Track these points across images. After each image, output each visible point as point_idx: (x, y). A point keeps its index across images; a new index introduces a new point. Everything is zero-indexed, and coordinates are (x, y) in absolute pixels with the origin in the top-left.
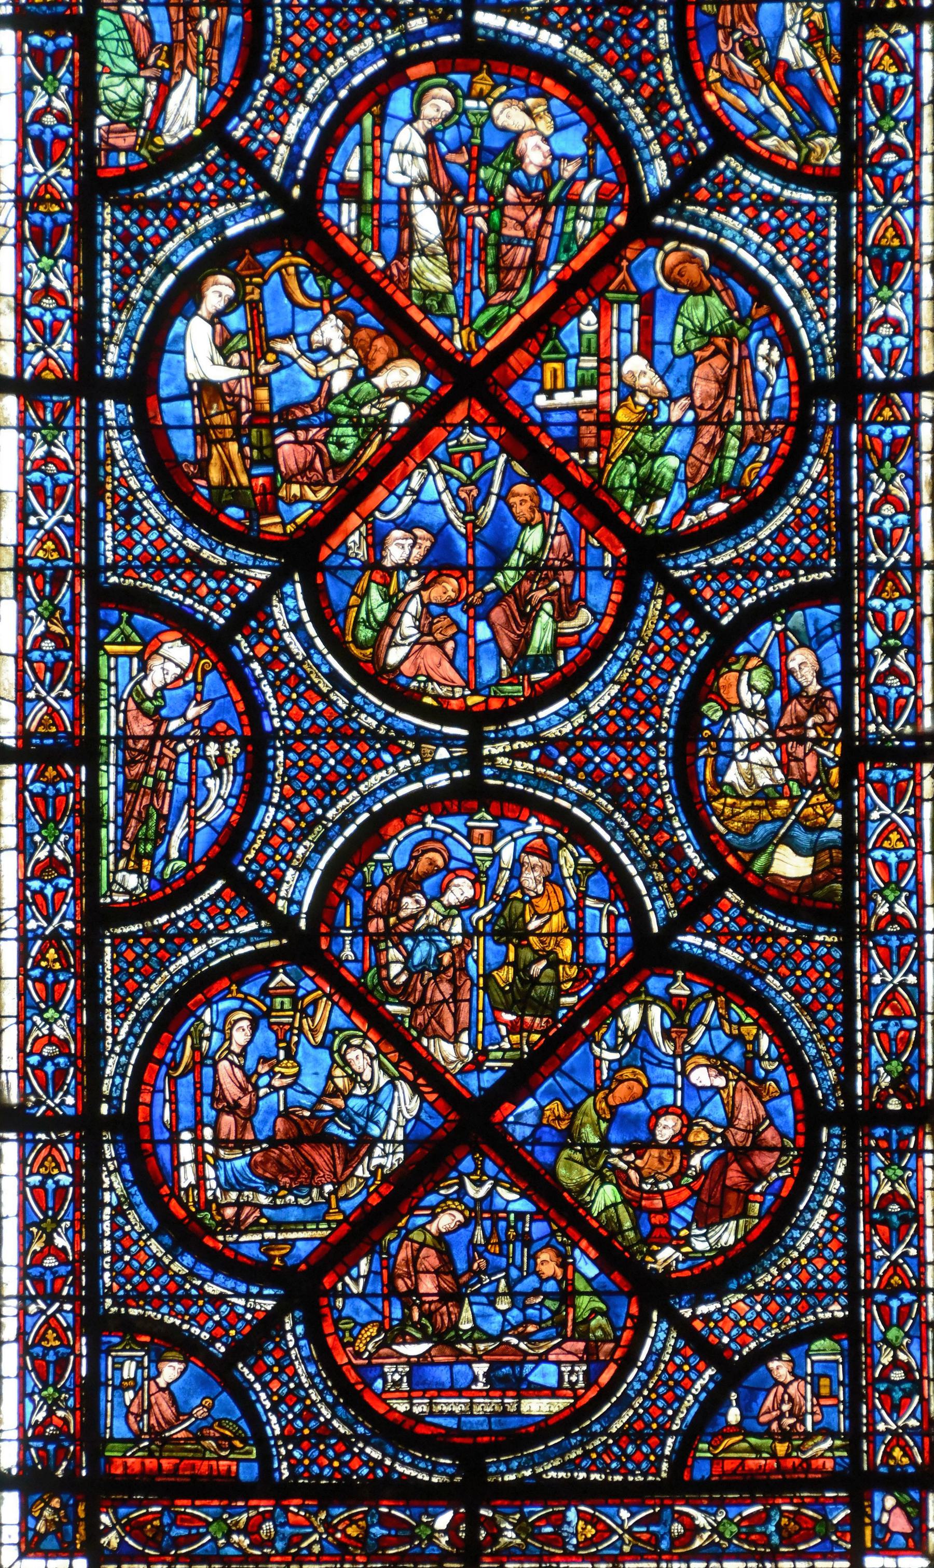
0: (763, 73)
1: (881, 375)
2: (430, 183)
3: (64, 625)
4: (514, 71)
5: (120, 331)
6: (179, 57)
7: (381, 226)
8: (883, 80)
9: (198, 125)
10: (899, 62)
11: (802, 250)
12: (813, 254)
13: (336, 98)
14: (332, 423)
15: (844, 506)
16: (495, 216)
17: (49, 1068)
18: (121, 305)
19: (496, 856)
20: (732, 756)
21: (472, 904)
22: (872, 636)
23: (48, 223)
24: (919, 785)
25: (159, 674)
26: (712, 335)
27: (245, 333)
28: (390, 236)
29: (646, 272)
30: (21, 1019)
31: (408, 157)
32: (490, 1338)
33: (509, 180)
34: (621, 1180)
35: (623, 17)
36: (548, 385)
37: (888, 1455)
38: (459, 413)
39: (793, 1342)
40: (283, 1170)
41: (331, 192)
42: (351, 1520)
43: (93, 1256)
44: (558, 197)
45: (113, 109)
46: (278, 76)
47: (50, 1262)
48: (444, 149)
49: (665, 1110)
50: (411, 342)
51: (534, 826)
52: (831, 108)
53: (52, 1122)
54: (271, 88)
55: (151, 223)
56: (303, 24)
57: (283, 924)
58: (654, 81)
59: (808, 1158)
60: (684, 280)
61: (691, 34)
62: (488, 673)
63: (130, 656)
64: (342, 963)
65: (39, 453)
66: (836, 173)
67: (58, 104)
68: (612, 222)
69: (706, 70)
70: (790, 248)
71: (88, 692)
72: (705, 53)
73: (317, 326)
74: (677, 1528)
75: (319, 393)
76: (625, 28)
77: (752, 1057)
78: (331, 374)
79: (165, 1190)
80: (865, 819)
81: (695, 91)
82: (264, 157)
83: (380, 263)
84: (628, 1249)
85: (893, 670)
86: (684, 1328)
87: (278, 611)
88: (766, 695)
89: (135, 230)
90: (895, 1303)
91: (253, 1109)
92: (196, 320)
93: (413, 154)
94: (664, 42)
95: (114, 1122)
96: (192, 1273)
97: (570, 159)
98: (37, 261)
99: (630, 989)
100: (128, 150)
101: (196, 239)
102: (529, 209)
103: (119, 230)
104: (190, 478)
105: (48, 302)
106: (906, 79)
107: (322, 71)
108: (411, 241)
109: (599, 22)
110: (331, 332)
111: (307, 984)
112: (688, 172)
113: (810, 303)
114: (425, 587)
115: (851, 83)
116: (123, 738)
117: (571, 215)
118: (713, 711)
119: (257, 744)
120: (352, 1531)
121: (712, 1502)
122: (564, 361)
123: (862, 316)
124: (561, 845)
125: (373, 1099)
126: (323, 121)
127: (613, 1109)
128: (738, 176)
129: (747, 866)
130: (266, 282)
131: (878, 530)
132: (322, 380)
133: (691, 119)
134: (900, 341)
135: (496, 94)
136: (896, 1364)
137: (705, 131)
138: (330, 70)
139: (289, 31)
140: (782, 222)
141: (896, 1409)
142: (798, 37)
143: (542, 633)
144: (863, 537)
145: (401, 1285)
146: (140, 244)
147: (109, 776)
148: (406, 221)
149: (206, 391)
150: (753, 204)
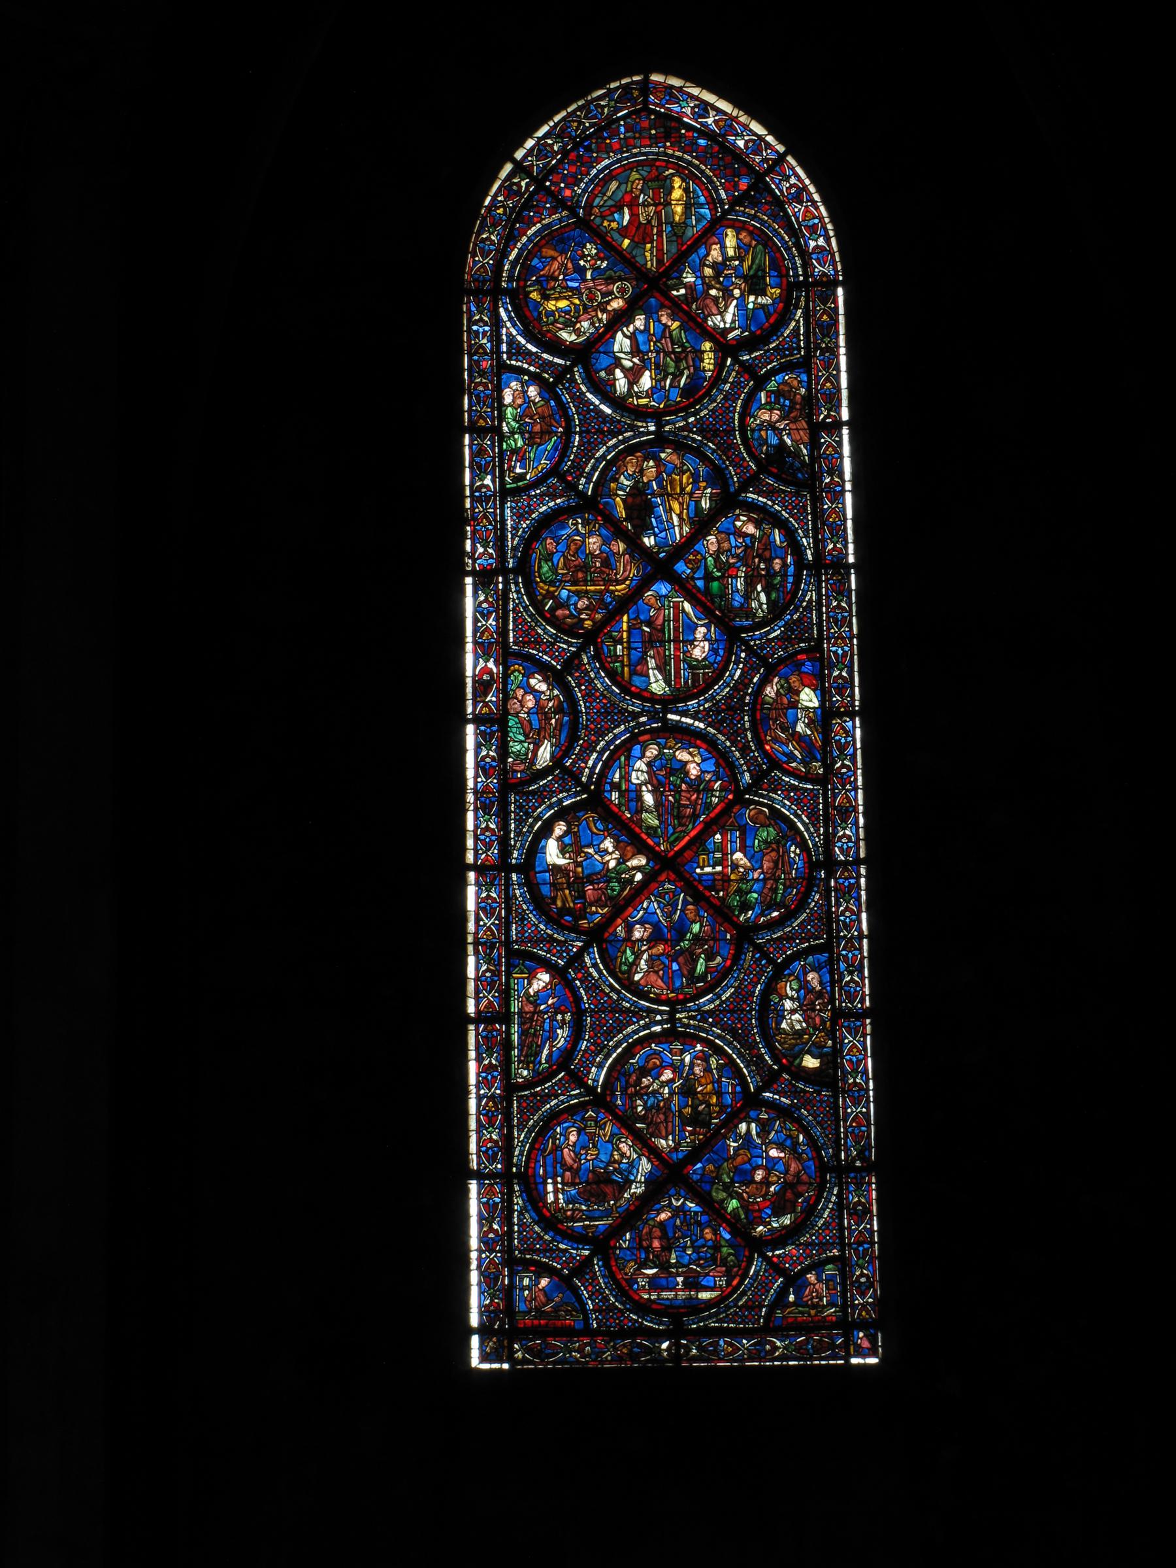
3: (495, 966)
5: (518, 845)
6: (542, 734)
7: (630, 800)
10: (847, 732)
14: (609, 881)
15: (829, 912)
17: (490, 1152)
18: (519, 833)
19: (682, 1060)
20: (784, 1017)
21: (672, 1081)
22: (843, 966)
24: (865, 1028)
25: (536, 986)
26: (770, 843)
30: (478, 1132)
32: (683, 1266)
33: (683, 781)
34: (739, 1197)
37: (860, 1314)
38: (663, 877)
39: (818, 1266)
40: (592, 1195)
41: (607, 787)
42: (624, 1346)
43: (510, 1232)
47: (491, 1235)
49: (759, 1167)
50: (641, 848)
51: (699, 1047)
53: (492, 1175)
57: (591, 1090)
59: (821, 1188)
62: (678, 984)
63: (524, 978)
64: (617, 1106)
65: (484, 895)
67: (492, 753)
71: (506, 995)
73: (602, 842)
74: (768, 1347)
77: (796, 1143)
79: (541, 1204)
80: (842, 1043)
81: (760, 745)
84: (743, 1227)
85: (852, 980)
86: (768, 1260)
87: (587, 959)
88: (798, 991)
90: (861, 1249)
91: (579, 1168)
94: (747, 725)
95: (519, 1175)
96: (553, 1240)
99: (741, 1116)
100: (521, 772)
101: (550, 807)
104: (548, 904)
108: (642, 806)
110: (608, 844)
111: (602, 1115)
114: (649, 948)
116: (521, 1013)
118: (775, 999)
119: (579, 1014)
120: (625, 1351)
121: (783, 1336)
123: (834, 834)
124: (711, 1056)
125: (632, 1164)
127: (736, 1167)
129: (792, 1063)
131: (844, 922)
134: (850, 844)
136: (862, 1275)
141: (863, 1295)
143: (701, 967)
144: (837, 925)
145: (644, 1244)
147: (515, 1028)
148: (639, 798)
149: (556, 869)
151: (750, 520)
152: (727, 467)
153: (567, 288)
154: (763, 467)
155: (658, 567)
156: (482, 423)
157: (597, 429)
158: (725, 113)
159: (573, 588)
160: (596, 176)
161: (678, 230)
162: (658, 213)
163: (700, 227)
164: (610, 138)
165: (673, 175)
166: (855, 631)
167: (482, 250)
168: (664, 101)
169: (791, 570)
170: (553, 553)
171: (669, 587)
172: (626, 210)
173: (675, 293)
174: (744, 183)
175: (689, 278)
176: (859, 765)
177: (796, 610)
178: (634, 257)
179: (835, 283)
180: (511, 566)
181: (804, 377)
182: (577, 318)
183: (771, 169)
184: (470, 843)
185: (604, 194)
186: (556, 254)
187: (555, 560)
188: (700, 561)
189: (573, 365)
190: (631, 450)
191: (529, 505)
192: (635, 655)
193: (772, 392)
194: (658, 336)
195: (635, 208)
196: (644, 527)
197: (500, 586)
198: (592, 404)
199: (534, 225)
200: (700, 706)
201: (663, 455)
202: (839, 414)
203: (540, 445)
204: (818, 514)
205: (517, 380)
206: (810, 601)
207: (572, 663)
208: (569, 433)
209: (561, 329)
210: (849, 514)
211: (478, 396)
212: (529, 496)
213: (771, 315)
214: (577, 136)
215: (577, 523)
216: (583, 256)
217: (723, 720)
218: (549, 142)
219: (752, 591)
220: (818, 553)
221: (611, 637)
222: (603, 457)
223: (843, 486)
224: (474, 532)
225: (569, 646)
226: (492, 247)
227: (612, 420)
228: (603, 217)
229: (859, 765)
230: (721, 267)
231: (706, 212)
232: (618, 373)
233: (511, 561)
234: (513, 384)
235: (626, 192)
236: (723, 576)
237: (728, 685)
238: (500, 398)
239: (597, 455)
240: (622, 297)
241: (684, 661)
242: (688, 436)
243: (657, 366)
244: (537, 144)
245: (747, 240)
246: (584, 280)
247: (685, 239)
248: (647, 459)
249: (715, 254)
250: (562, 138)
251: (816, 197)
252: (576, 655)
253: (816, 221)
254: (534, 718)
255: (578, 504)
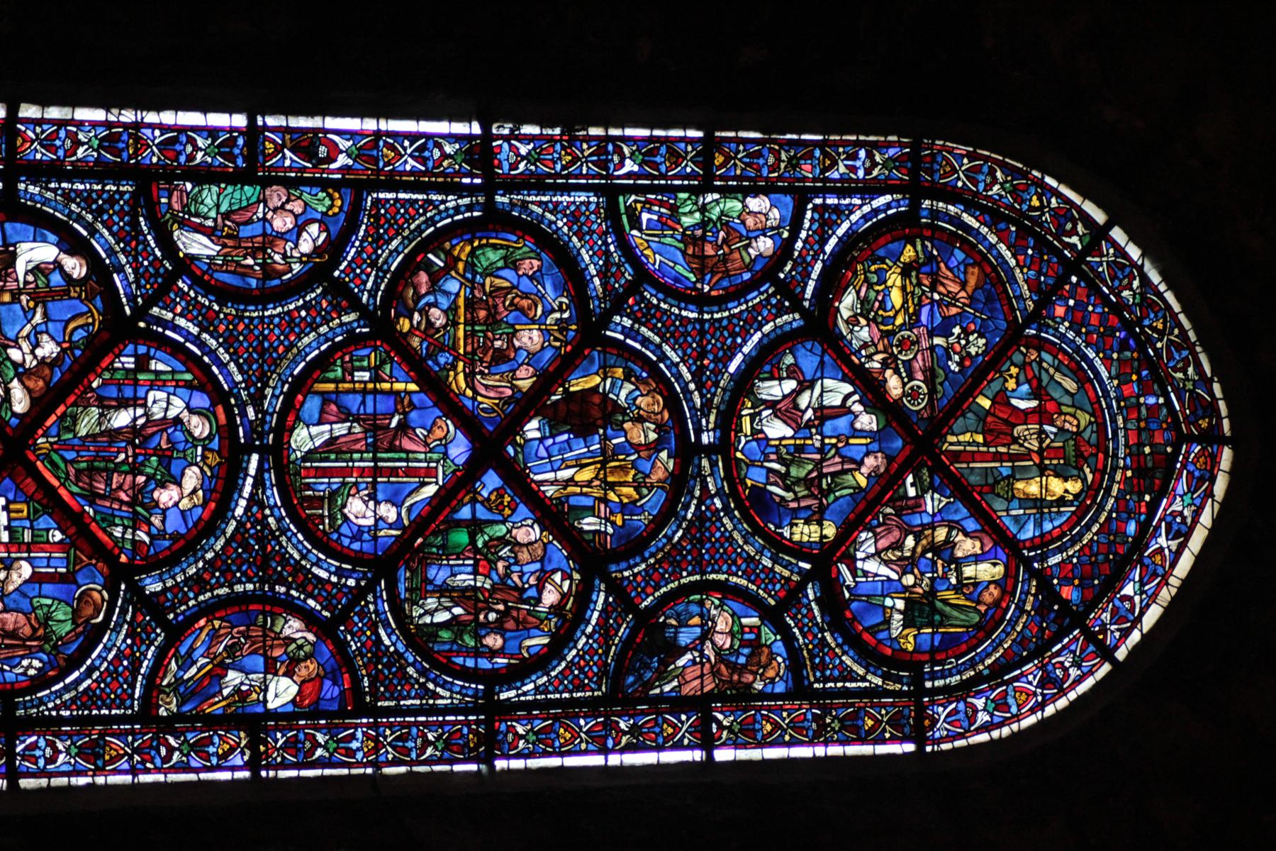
0: (219, 659)
1: (18, 749)
2: (148, 421)
4: (220, 482)
5: (49, 195)
6: (230, 242)
7: (120, 386)
8: (213, 744)
9: (186, 255)
10: (225, 756)
11: (102, 690)
12: (99, 698)
13: (203, 354)
16: (125, 468)
18: (68, 197)
23: (121, 145)
26: (46, 626)
27: (48, 286)
28: (112, 392)
29: (87, 577)
31: (165, 405)
33: (150, 478)
35: (255, 558)
36: (12, 507)
41: (142, 350)
44: (139, 513)
45: (196, 195)
46: (218, 313)
48: (170, 431)
50: (41, 405)
52: (195, 708)
54: (210, 308)
55: (121, 220)
56: (252, 331)
58: (213, 581)
60: (82, 604)
61: (244, 608)
66: (154, 712)
67: (200, 155)
68: (121, 552)
69: (222, 619)
70: (104, 681)
72: (231, 617)
73: (53, 338)
75: (7, 339)
76: (247, 560)
78: (20, 348)
81: (207, 610)
82: (164, 302)
83: (95, 385)
89: (117, 208)
92: (55, 251)
93: (166, 410)
94: (239, 588)
97: (163, 522)
98: (96, 136)
100: (169, 204)
101: (111, 252)
102: (130, 492)
103: (117, 197)
105: (68, 142)
106: (214, 761)
107: (220, 345)
108: (109, 407)
109: (252, 542)
110: (48, 349)
112: (154, 606)
113: (67, 697)
115: (213, 722)
117: (126, 522)
122: (28, 518)
123: (58, 735)
126: (188, 344)
128: (152, 643)
130: (82, 301)
132: (16, 341)
133: (189, 608)
134: (41, 762)
135: (206, 468)
137: (181, 618)
138: (221, 350)
139: (246, 321)
140: (121, 675)
142: (242, 683)
146: (107, 212)
148: (123, 404)
150: (133, 654)
151: (564, 597)
152: (644, 560)
153: (920, 305)
154: (646, 620)
155: (492, 444)
156: (719, 159)
157: (706, 348)
158: (1173, 565)
159: (461, 302)
160: (1085, 357)
161: (1000, 485)
162: (1027, 456)
163: (1007, 521)
164: (1139, 380)
165: (1084, 480)
166: (388, 771)
167: (978, 170)
168: (1191, 468)
169: (484, 664)
170: (516, 269)
171: (461, 460)
172: (1034, 404)
173: (910, 479)
174: (1069, 593)
175: (931, 503)
176: (173, 777)
177: (423, 672)
178: (963, 415)
179: (921, 741)
180: (498, 199)
181: (780, 688)
182: (874, 320)
183: (1090, 637)
184: (54, 113)
185: (1057, 370)
186: (969, 289)
187: (507, 273)
188: (501, 512)
189: (804, 313)
190: (672, 403)
191: (591, 232)
192: (353, 402)
193: (759, 636)
194: (845, 452)
195: (1036, 417)
196: (557, 420)
197: (466, 181)
198: (745, 342)
199: (1014, 256)
200: (271, 508)
201: (664, 455)
202: (724, 745)
203: (684, 253)
204: (570, 709)
205: (782, 219)
206: (436, 696)
207: (342, 295)
208: (701, 301)
209: (858, 293)
210: (571, 761)
211: (758, 154)
212: (606, 233)
213: (874, 634)
214: (1142, 328)
215: (561, 310)
216: (966, 332)
217: (248, 548)
218: (1136, 284)
219: (452, 599)
220: (509, 709)
221: (383, 362)
222: (663, 357)
223: (613, 751)
224: (551, 139)
225: (369, 288)
226: (981, 186)
227: (718, 373)
228: (1023, 367)
229: (173, 777)
230: (946, 555)
231: (1029, 532)
232: (790, 385)
233: (506, 200)
234: (775, 213)
235: (1060, 404)
236: (476, 551)
237: (304, 557)
238: (755, 191)
239: (666, 348)
240: (904, 394)
241: (344, 484)
242: (693, 497)
243: (800, 449)
244: (1133, 264)
245: (987, 598)
246: (931, 335)
247: (989, 497)
248: (659, 428)
249: (967, 546)
250: (1140, 305)
251: (1050, 710)
252: (355, 304)
253: (1014, 710)
254: (256, 229)
255: (590, 313)
